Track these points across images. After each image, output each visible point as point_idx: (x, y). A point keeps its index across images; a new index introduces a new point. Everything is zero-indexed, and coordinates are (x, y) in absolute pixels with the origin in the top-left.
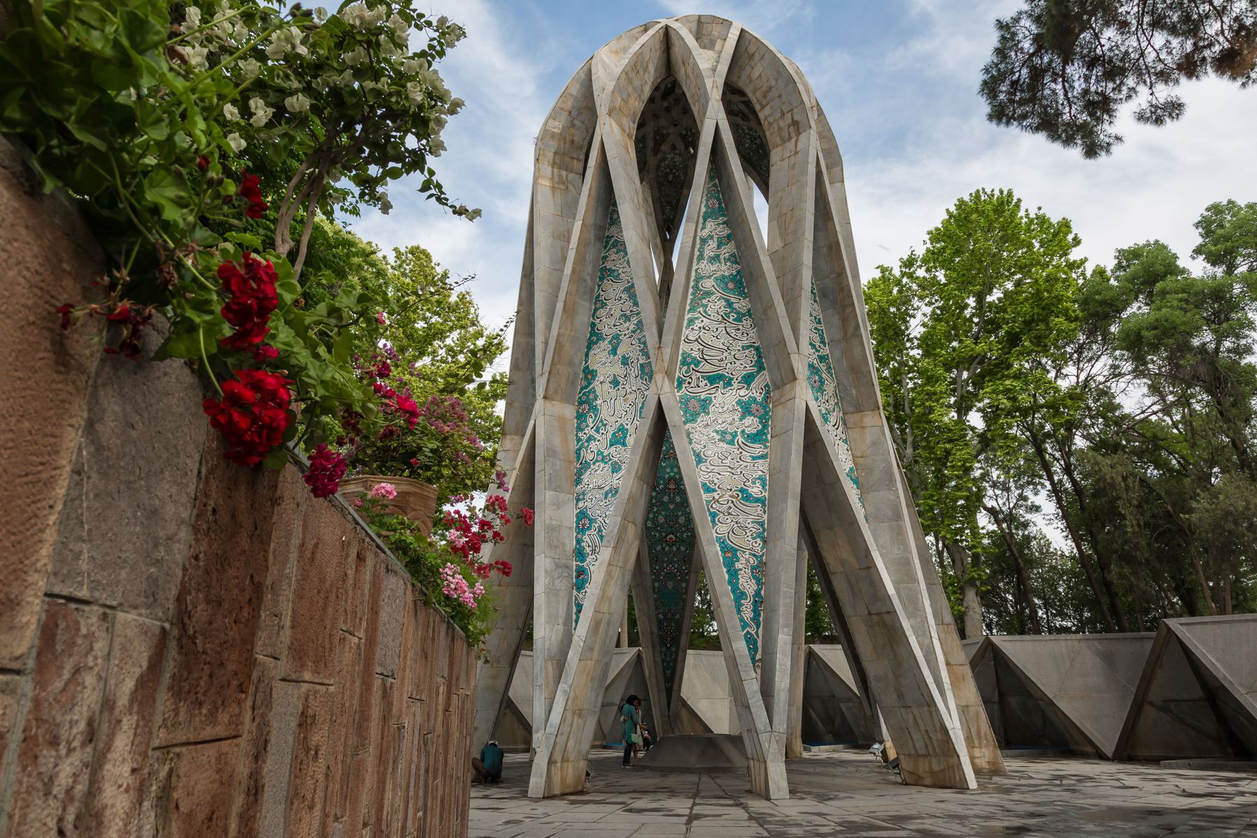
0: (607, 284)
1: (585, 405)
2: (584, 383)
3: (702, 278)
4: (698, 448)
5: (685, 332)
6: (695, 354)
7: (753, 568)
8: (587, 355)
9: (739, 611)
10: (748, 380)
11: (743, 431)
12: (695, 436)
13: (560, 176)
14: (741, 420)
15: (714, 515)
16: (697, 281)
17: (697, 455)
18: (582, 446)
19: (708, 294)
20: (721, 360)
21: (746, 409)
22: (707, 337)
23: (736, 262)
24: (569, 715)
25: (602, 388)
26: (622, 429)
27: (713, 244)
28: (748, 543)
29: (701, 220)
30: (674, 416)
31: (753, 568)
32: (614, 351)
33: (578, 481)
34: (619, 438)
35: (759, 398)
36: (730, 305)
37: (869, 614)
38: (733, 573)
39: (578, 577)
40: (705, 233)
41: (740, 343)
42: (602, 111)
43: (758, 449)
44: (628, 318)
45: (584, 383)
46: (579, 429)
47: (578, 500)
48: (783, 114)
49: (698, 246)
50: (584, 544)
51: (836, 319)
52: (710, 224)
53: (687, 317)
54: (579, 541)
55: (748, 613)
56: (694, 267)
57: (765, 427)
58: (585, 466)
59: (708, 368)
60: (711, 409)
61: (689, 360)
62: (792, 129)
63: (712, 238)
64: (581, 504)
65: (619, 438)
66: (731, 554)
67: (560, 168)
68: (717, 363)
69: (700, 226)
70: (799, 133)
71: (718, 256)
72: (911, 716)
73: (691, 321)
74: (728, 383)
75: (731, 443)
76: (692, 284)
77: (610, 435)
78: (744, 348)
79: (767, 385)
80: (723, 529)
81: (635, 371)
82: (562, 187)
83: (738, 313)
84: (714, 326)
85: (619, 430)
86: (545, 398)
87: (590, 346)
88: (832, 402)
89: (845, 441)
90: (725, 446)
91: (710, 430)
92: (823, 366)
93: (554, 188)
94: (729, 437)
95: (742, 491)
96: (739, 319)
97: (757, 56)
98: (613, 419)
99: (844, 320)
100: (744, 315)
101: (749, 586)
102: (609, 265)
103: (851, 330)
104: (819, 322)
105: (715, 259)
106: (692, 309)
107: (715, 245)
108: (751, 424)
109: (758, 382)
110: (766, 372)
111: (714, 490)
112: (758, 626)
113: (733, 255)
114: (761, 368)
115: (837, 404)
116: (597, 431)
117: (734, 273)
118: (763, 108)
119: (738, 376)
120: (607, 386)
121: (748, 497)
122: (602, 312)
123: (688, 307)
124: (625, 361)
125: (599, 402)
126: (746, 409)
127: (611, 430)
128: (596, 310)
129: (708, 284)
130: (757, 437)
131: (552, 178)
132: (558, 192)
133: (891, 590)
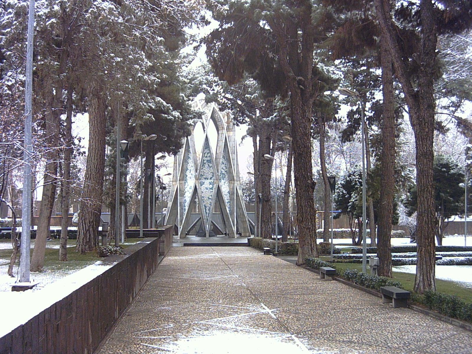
0: (189, 160)
10: (211, 178)
22: (204, 171)
27: (206, 154)
28: (208, 205)
30: (197, 187)
36: (209, 165)
52: (206, 150)
55: (207, 216)
58: (186, 192)
74: (208, 179)
101: (208, 212)
105: (206, 157)
109: (212, 179)
119: (209, 178)
121: (209, 198)
124: (192, 174)
129: (205, 162)
130: (212, 189)
133: (228, 212)
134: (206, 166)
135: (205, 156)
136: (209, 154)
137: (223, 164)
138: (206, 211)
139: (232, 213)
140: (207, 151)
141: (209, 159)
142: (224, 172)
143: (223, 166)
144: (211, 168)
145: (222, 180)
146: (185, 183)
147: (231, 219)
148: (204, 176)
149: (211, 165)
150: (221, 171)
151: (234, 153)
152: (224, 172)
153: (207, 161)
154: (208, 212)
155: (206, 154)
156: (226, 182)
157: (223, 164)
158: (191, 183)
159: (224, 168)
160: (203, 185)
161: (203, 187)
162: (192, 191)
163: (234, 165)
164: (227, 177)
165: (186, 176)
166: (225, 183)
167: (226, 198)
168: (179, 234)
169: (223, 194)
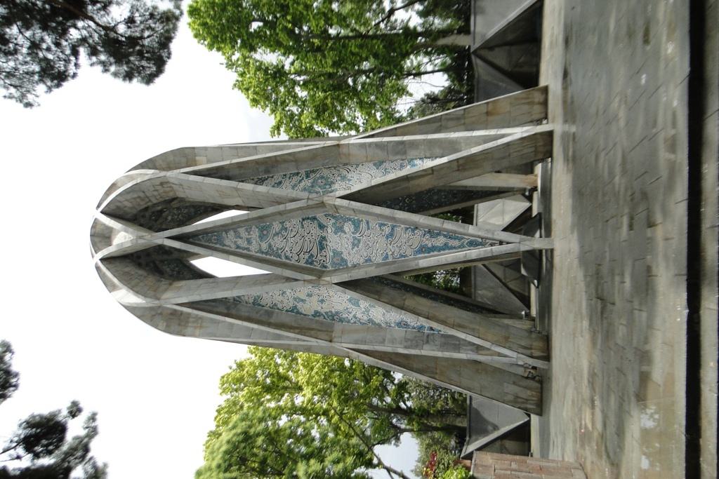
0: (262, 303)
1: (334, 317)
2: (322, 317)
3: (260, 249)
4: (362, 260)
5: (293, 262)
6: (307, 256)
7: (431, 237)
8: (305, 315)
9: (455, 248)
10: (322, 227)
11: (353, 233)
12: (355, 261)
13: (193, 322)
14: (345, 233)
15: (402, 256)
16: (263, 253)
17: (366, 261)
18: (359, 321)
19: (270, 246)
20: (310, 241)
21: (339, 229)
23: (251, 228)
24: (507, 345)
25: (325, 308)
26: (350, 300)
28: (417, 239)
29: (225, 248)
30: (345, 277)
31: (431, 237)
32: (303, 301)
33: (379, 325)
35: (333, 221)
36: (277, 234)
37: (458, 170)
38: (433, 249)
39: (433, 330)
40: (233, 246)
41: (300, 229)
42: (157, 303)
43: (363, 225)
44: (284, 293)
45: (322, 317)
46: (349, 322)
47: (390, 326)
48: (157, 190)
49: (241, 251)
50: (415, 326)
51: (283, 166)
52: (227, 242)
53: (284, 260)
54: (415, 328)
55: (456, 243)
56: (254, 253)
57: (350, 220)
58: (370, 321)
59: (314, 251)
60: (339, 250)
61: (310, 261)
62: (165, 186)
63: (235, 242)
64: (393, 325)
66: (424, 249)
67: (187, 322)
68: (312, 244)
69: (228, 248)
70: (168, 182)
71: (247, 239)
72: (515, 154)
73: (287, 258)
74: (324, 238)
75: (359, 241)
76: (264, 256)
77: (353, 307)
78: (303, 227)
79: (326, 215)
80: (409, 252)
81: (316, 291)
82: (200, 321)
83: (282, 230)
84: (289, 243)
85: (350, 301)
86: (331, 341)
87: (298, 313)
88: (334, 171)
89: (357, 165)
90: (361, 244)
91: (352, 252)
92: (312, 176)
93: (201, 327)
94: (356, 242)
95: (387, 238)
96: (286, 228)
97: (119, 204)
98: (344, 304)
99: (285, 161)
100: (283, 226)
101: (441, 241)
102: (251, 301)
103: (291, 158)
104: (285, 175)
105: (249, 241)
106: (280, 256)
107: (240, 240)
108: (348, 227)
109: (323, 221)
110: (318, 216)
111: (387, 254)
112: (462, 238)
113: (247, 229)
114: (315, 218)
115: (335, 168)
116: (350, 313)
117: (257, 230)
118: (150, 201)
120: (324, 306)
121: (391, 235)
122: (280, 306)
123: (278, 259)
124: (310, 295)
125: (333, 310)
126: (339, 229)
127: (350, 306)
128: (278, 309)
129: (264, 246)
130: (357, 225)
131: (195, 328)
132: (204, 324)
133: (445, 160)
134: (278, 242)
135: (245, 245)
137: (280, 183)
138: (440, 249)
141: (255, 233)
144: (287, 224)
146: (341, 320)
148: (314, 251)
149: (276, 227)
151: (256, 147)
152: (307, 183)
153: (261, 237)
155: (240, 242)
156: (345, 173)
157: (280, 183)
158: (341, 301)
159: (296, 179)
160: (345, 256)
161: (353, 257)
165: (317, 314)
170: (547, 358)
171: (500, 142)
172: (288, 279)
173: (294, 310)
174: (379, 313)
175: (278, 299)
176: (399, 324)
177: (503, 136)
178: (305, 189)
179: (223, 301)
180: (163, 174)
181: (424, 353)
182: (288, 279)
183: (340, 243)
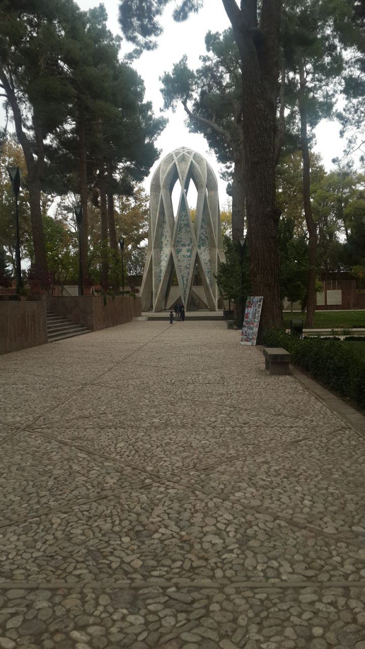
1: (161, 248)
21: (188, 251)
22: (182, 237)
25: (164, 246)
27: (183, 217)
28: (186, 275)
30: (174, 255)
34: (166, 257)
38: (183, 280)
42: (162, 186)
65: (166, 257)
66: (183, 277)
105: (183, 220)
121: (187, 267)
129: (182, 226)
130: (190, 256)
133: (208, 282)
134: (183, 230)
136: (186, 218)
139: (212, 285)
140: (183, 213)
141: (186, 222)
142: (203, 237)
143: (203, 231)
145: (202, 248)
146: (161, 251)
147: (211, 291)
150: (201, 237)
153: (185, 225)
154: (186, 283)
155: (183, 217)
158: (167, 251)
159: (205, 233)
162: (166, 259)
163: (215, 228)
164: (207, 243)
165: (162, 243)
166: (205, 250)
167: (205, 268)
168: (154, 308)
169: (202, 262)
170: (155, 312)
171: (213, 298)
172: (172, 235)
173: (162, 235)
174: (164, 264)
175: (166, 230)
176: (161, 270)
177: (215, 298)
178: (201, 238)
179: (164, 211)
180: (205, 186)
181: (153, 279)
182: (172, 235)
183: (184, 251)
